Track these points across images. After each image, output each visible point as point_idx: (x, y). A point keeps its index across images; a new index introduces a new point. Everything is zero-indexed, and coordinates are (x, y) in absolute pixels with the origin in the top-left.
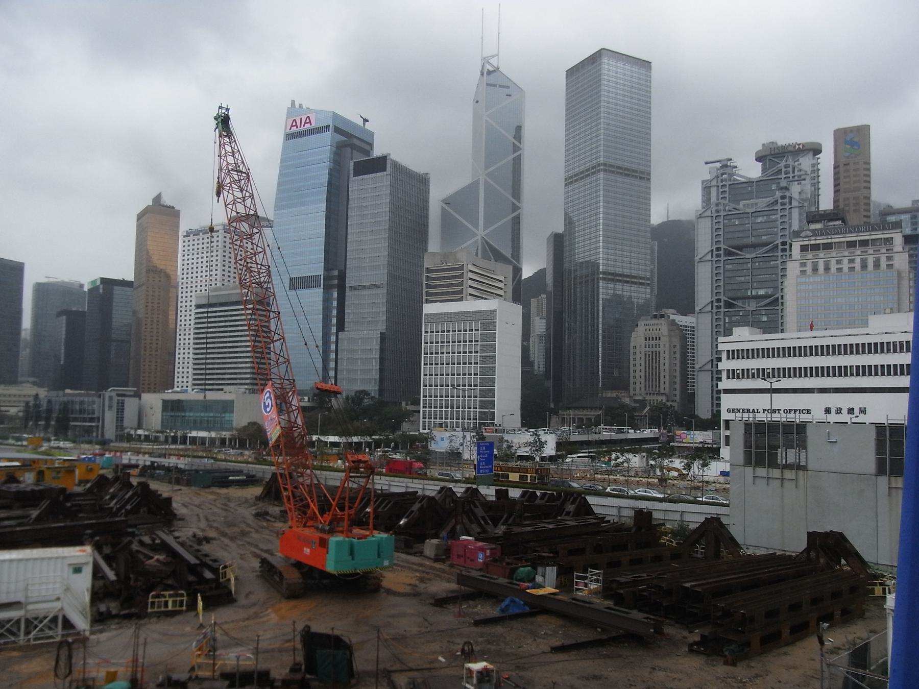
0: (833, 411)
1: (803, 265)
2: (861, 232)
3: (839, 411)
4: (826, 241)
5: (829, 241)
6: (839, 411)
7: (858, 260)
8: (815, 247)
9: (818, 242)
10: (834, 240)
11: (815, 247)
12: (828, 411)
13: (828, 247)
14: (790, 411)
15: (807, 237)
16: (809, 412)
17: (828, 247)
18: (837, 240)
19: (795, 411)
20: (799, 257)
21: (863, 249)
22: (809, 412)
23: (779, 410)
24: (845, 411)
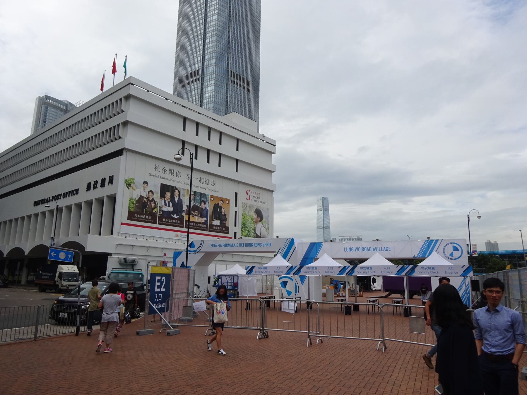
14: (67, 193)
23: (61, 195)
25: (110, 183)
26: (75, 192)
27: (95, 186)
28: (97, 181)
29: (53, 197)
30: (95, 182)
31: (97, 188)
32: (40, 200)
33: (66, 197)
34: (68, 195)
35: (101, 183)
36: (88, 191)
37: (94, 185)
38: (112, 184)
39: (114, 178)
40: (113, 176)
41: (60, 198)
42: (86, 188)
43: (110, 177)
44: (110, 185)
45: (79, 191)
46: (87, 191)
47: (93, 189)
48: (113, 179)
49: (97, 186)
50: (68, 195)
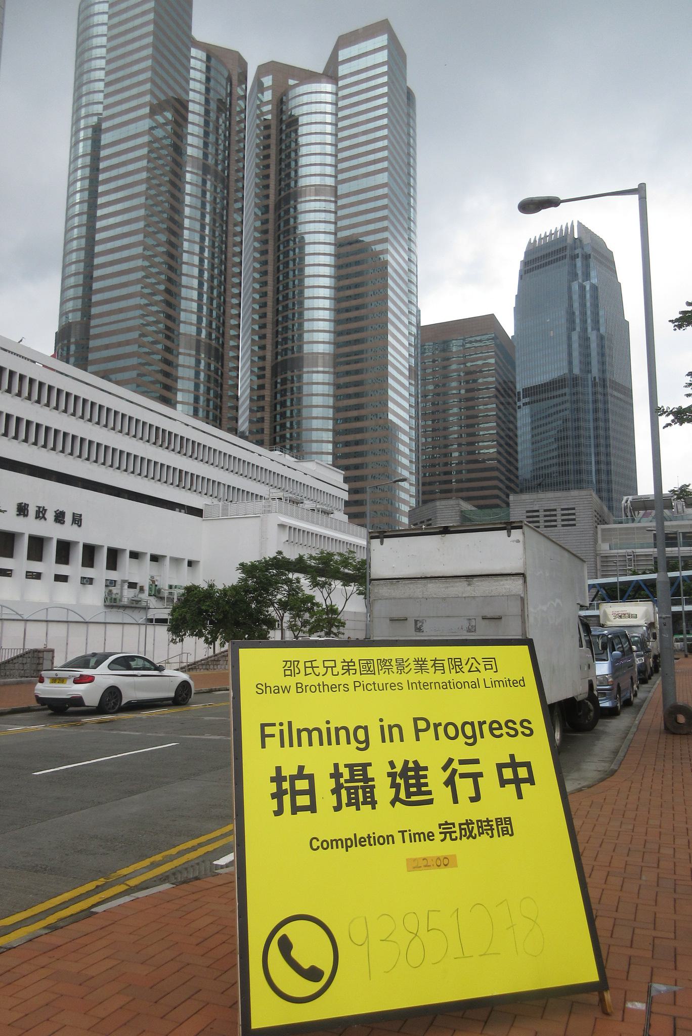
0: (32, 511)
3: (41, 513)
6: (41, 513)
12: (22, 510)
24: (50, 516)
25: (75, 523)
27: (41, 515)
28: (44, 507)
30: (39, 507)
31: (45, 519)
36: (22, 517)
37: (38, 512)
38: (80, 526)
39: (82, 517)
40: (81, 515)
42: (16, 510)
43: (74, 514)
44: (75, 526)
46: (17, 515)
47: (36, 518)
48: (81, 519)
49: (46, 516)
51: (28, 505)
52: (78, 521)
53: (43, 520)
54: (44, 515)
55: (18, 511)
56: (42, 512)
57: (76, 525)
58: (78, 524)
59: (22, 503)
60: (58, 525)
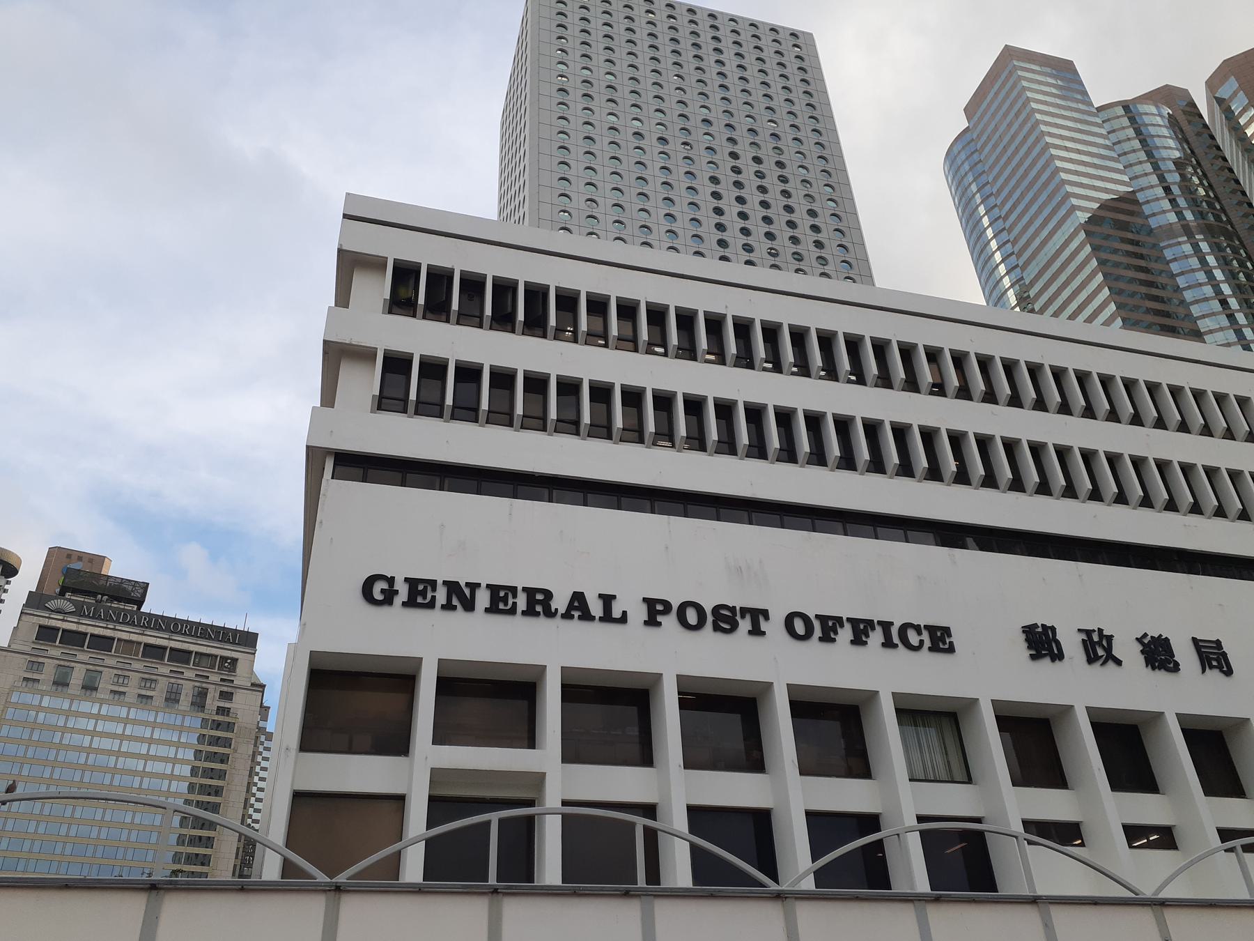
1: (35, 666)
2: (180, 633)
4: (97, 631)
5: (108, 633)
7: (163, 684)
8: (73, 639)
9: (82, 629)
10: (118, 635)
11: (73, 639)
13: (102, 643)
15: (58, 611)
16: (940, 640)
17: (102, 643)
18: (125, 636)
19: (861, 630)
20: (27, 649)
21: (176, 667)
22: (940, 640)
23: (757, 616)
25: (1211, 667)
26: (913, 638)
27: (1100, 652)
28: (1100, 631)
29: (655, 610)
30: (1089, 633)
32: (474, 587)
33: (827, 638)
34: (845, 634)
35: (1142, 652)
36: (1046, 661)
40: (1218, 643)
41: (756, 631)
42: (1026, 645)
43: (1195, 640)
44: (1214, 675)
45: (956, 639)
48: (1224, 655)
49: (1115, 652)
50: (845, 634)
51: (1053, 629)
52: (1218, 660)
53: (1111, 664)
54: (1109, 650)
55: (1029, 648)
56: (1100, 643)
57: (1216, 672)
58: (1220, 668)
59: (1035, 626)
60: (1161, 675)
